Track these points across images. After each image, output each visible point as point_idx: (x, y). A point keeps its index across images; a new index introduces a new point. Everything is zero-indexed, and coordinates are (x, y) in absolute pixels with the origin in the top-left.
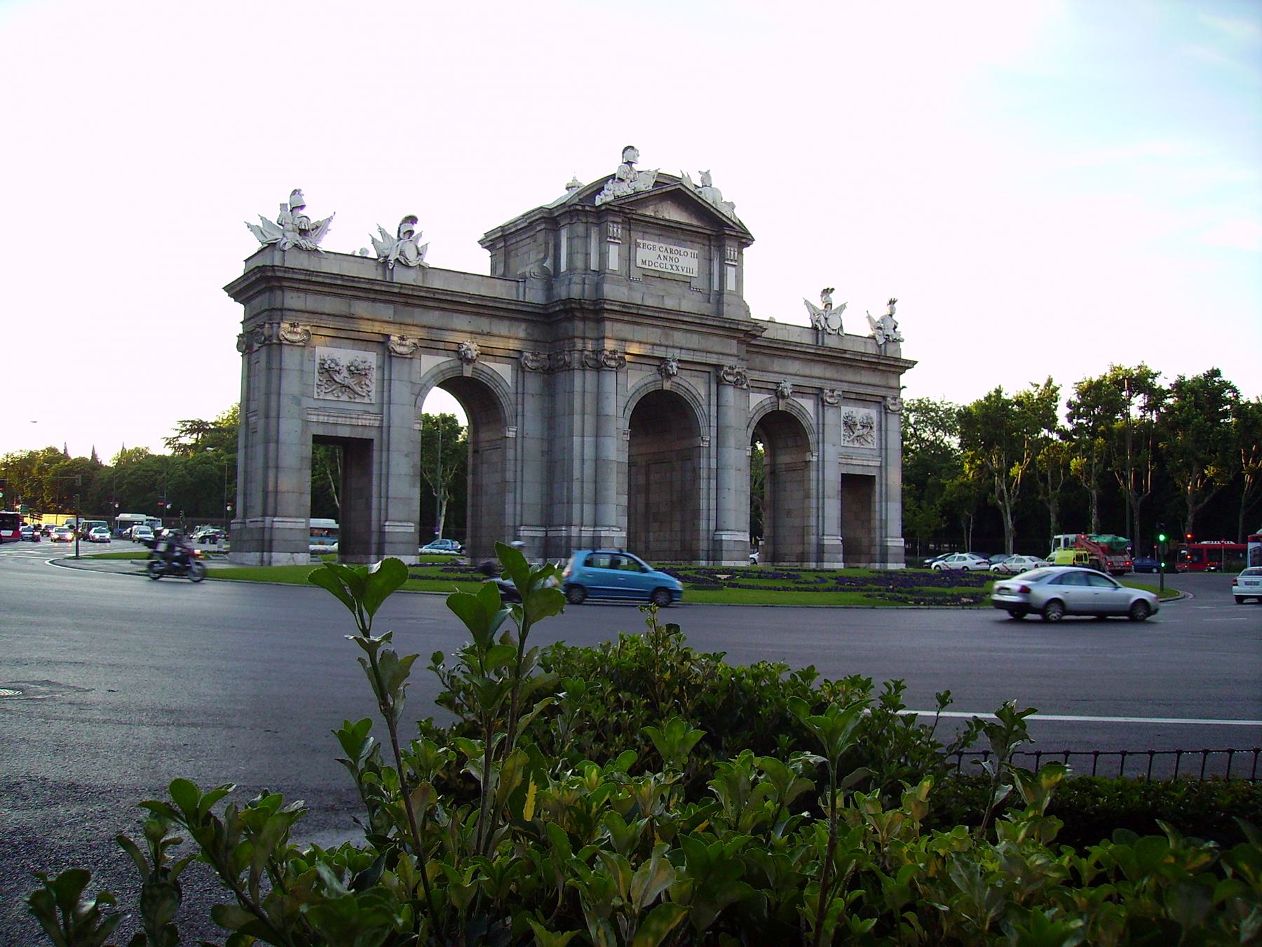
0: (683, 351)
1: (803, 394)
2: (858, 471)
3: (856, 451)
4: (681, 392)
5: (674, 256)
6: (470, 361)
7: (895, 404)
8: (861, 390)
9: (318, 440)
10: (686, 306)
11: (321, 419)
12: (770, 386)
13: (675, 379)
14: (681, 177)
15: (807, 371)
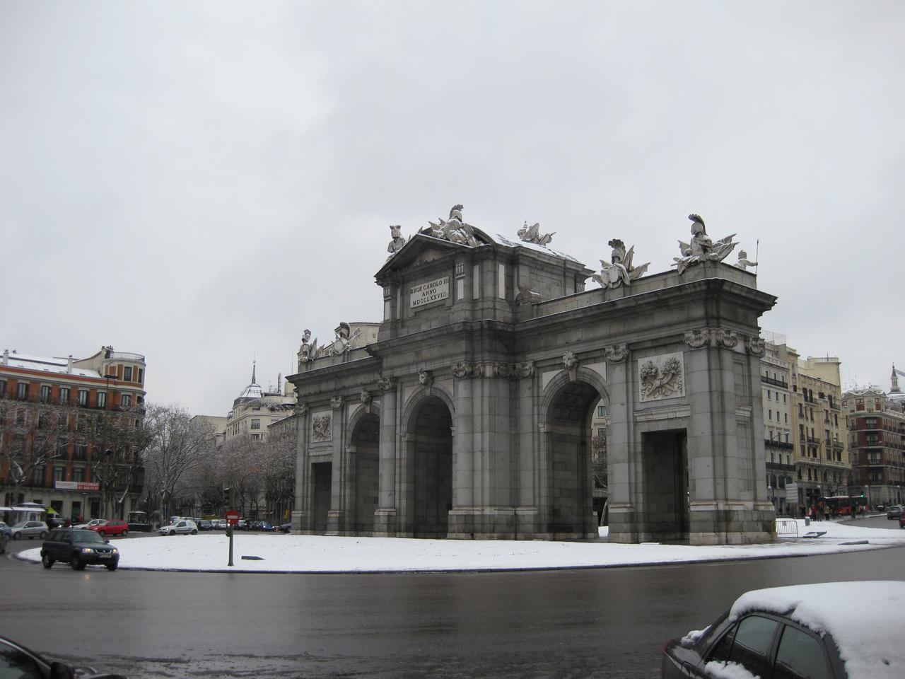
0: (428, 363)
1: (596, 360)
2: (663, 427)
3: (659, 404)
4: (439, 395)
5: (433, 289)
6: (366, 403)
7: (700, 338)
8: (654, 335)
9: (313, 464)
10: (435, 325)
11: (315, 454)
12: (558, 362)
13: (435, 385)
14: (430, 226)
15: (591, 335)
